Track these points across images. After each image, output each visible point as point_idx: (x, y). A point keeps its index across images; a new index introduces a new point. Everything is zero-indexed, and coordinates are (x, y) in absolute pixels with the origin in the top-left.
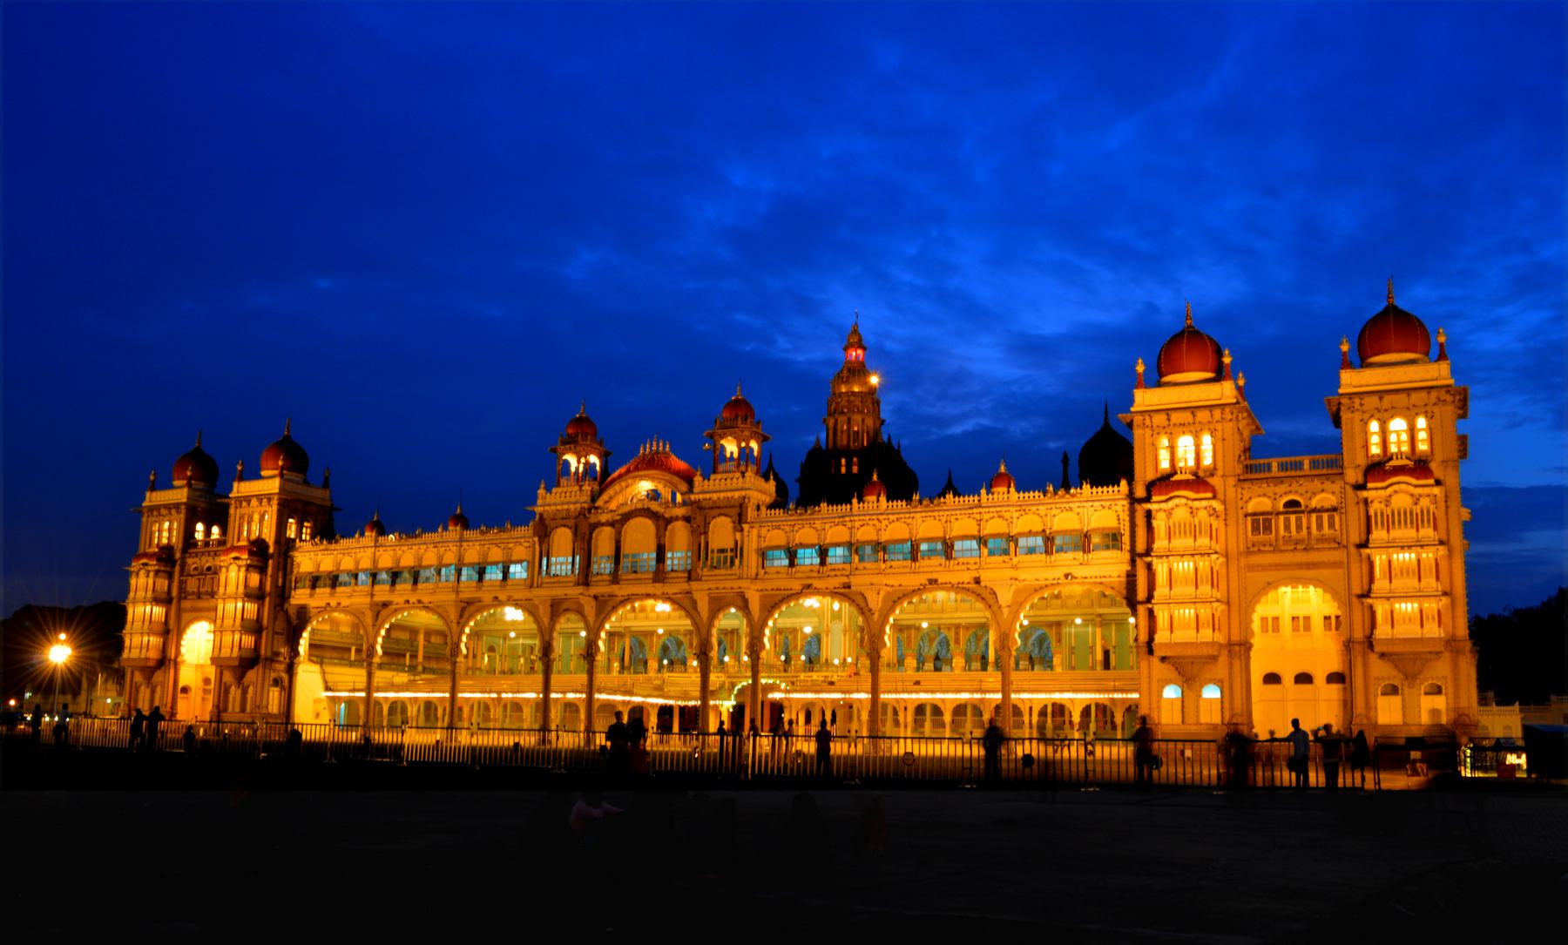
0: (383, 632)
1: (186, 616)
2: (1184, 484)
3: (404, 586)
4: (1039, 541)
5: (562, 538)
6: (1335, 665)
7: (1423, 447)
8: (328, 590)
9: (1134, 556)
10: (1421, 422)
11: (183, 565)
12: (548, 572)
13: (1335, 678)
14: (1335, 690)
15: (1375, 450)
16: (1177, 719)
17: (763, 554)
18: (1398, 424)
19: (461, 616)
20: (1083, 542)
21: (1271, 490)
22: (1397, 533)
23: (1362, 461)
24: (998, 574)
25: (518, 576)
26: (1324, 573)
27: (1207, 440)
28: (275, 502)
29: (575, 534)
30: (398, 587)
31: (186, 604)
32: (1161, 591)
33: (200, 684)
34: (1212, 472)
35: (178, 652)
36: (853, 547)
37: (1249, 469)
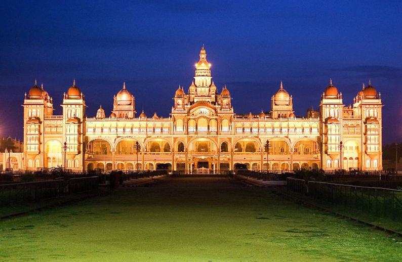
5: (180, 122)
9: (321, 134)
10: (375, 110)
13: (358, 158)
14: (357, 160)
15: (368, 116)
16: (330, 166)
18: (371, 111)
23: (365, 117)
26: (357, 139)
28: (82, 106)
32: (329, 142)
36: (259, 128)
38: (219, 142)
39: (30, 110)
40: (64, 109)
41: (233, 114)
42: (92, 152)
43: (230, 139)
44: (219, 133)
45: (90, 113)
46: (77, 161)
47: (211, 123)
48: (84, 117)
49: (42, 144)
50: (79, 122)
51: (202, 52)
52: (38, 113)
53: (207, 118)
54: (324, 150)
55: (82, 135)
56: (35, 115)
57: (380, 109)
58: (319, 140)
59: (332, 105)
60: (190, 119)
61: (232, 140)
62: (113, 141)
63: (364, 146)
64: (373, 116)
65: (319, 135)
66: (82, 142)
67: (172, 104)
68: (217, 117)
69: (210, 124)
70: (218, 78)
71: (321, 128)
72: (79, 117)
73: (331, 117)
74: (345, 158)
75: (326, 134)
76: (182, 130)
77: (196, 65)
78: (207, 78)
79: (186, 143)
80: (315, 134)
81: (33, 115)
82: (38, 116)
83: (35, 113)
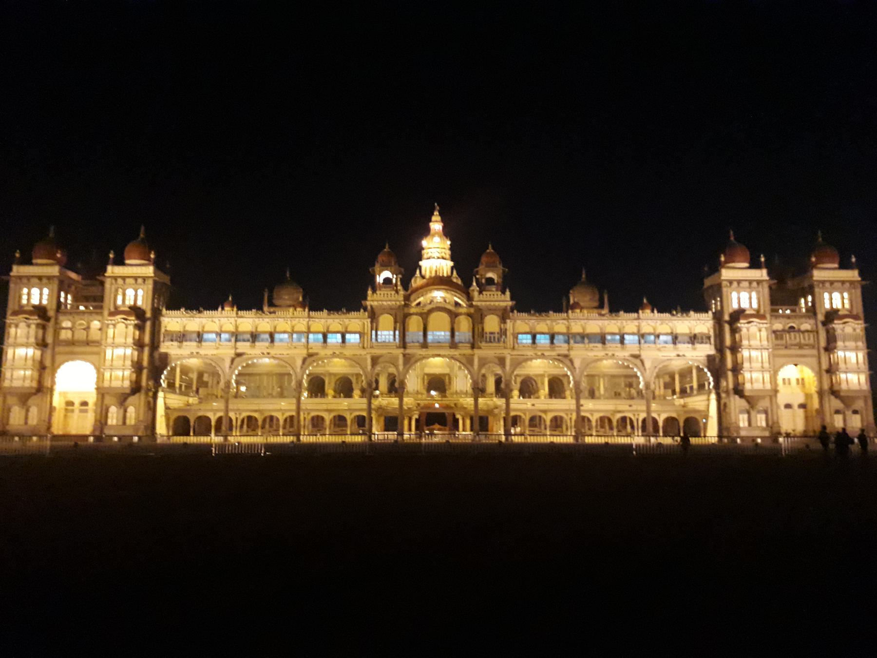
0: (236, 372)
1: (58, 358)
2: (752, 316)
3: (262, 346)
4: (669, 338)
5: (386, 320)
6: (801, 400)
8: (194, 344)
9: (720, 348)
10: (846, 295)
11: (57, 322)
12: (376, 340)
13: (803, 406)
14: (801, 412)
16: (746, 424)
17: (515, 336)
20: (694, 339)
21: (782, 320)
22: (848, 344)
23: (824, 312)
25: (352, 341)
26: (809, 360)
27: (754, 295)
30: (257, 344)
31: (59, 349)
32: (746, 365)
33: (63, 405)
34: (758, 311)
35: (53, 383)
41: (510, 303)
44: (476, 346)
46: (131, 410)
47: (459, 322)
51: (434, 218)
53: (448, 312)
57: (859, 292)
58: (716, 366)
61: (508, 362)
63: (825, 377)
64: (840, 307)
67: (370, 281)
68: (472, 310)
70: (465, 260)
72: (144, 307)
75: (735, 348)
76: (392, 337)
79: (401, 368)
80: (709, 349)
82: (45, 302)
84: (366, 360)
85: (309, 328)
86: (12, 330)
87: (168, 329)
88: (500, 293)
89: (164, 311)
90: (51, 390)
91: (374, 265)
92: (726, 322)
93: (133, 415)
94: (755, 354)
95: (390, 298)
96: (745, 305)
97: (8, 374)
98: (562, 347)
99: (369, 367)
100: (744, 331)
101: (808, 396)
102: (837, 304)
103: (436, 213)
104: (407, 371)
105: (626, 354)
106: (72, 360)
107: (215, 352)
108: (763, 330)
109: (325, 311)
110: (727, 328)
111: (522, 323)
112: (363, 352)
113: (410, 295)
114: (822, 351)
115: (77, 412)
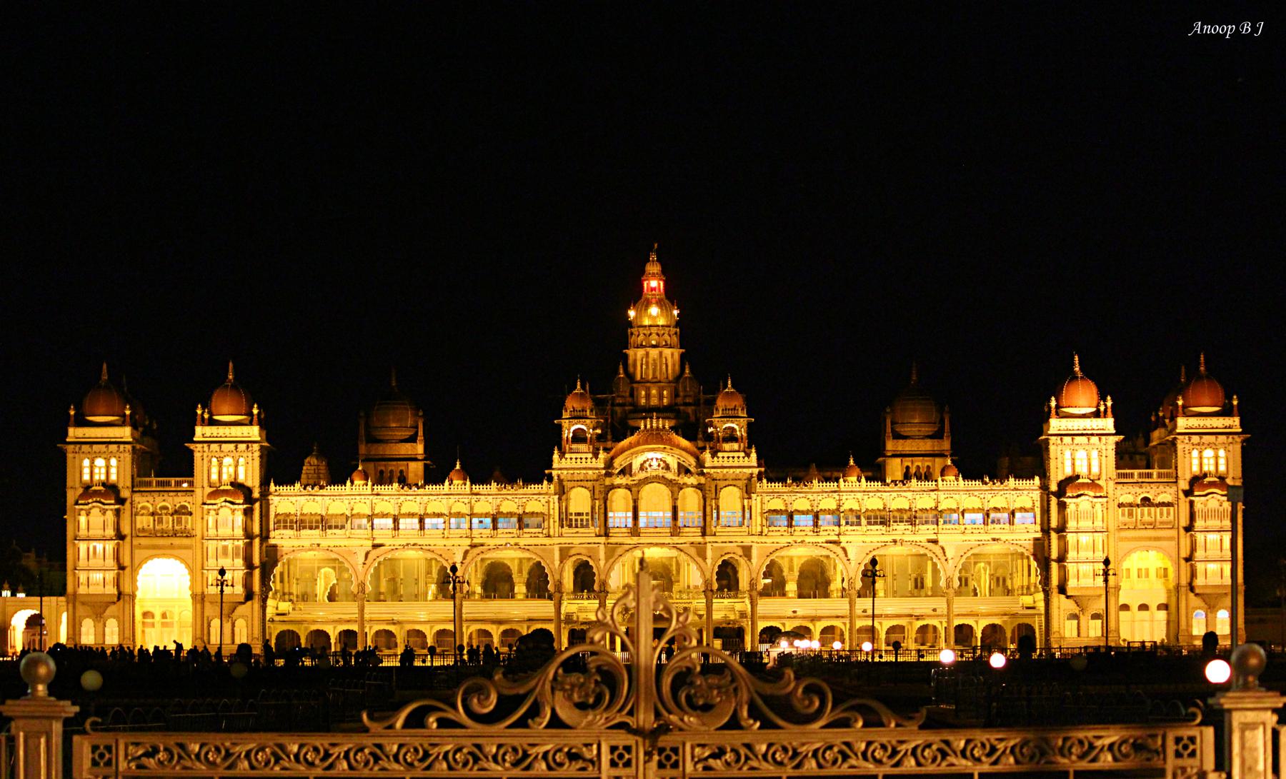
4: (980, 516)
6: (1163, 601)
7: (1222, 468)
9: (1046, 530)
13: (1164, 607)
14: (1162, 615)
15: (1196, 469)
16: (1075, 633)
18: (1208, 453)
19: (464, 558)
23: (1188, 477)
24: (953, 540)
26: (1164, 544)
28: (256, 447)
29: (593, 491)
31: (136, 542)
32: (1071, 555)
35: (135, 588)
37: (1119, 476)
38: (709, 561)
39: (86, 462)
40: (197, 455)
41: (756, 471)
42: (290, 594)
43: (747, 551)
45: (280, 467)
46: (240, 624)
47: (684, 498)
48: (264, 483)
49: (128, 571)
50: (249, 500)
52: (113, 471)
53: (669, 483)
54: (1055, 581)
55: (257, 541)
56: (103, 478)
57: (1238, 448)
58: (1041, 554)
59: (1081, 435)
60: (613, 487)
61: (754, 552)
62: (362, 559)
63: (1185, 567)
64: (1212, 469)
65: (1039, 535)
66: (256, 561)
67: (554, 439)
69: (679, 503)
71: (1046, 511)
72: (249, 484)
73: (1078, 477)
74: (1125, 607)
75: (1061, 529)
77: (632, 313)
78: (667, 352)
79: (602, 563)
80: (1026, 531)
81: (96, 477)
82: (113, 477)
83: (104, 471)
84: (552, 551)
85: (472, 508)
86: (83, 519)
87: (280, 511)
88: (742, 454)
89: (272, 487)
90: (133, 596)
91: (560, 417)
92: (1053, 493)
93: (244, 631)
94: (1085, 539)
95: (584, 465)
96: (1082, 469)
97: (82, 577)
98: (828, 531)
99: (557, 563)
100: (1071, 509)
101: (1169, 591)
102: (1209, 467)
103: (654, 257)
104: (610, 569)
105: (923, 538)
106: (157, 556)
107: (346, 542)
108: (1098, 507)
109: (494, 485)
110: (1054, 501)
111: (772, 496)
112: (547, 541)
113: (612, 458)
114: (1182, 531)
115: (158, 626)
